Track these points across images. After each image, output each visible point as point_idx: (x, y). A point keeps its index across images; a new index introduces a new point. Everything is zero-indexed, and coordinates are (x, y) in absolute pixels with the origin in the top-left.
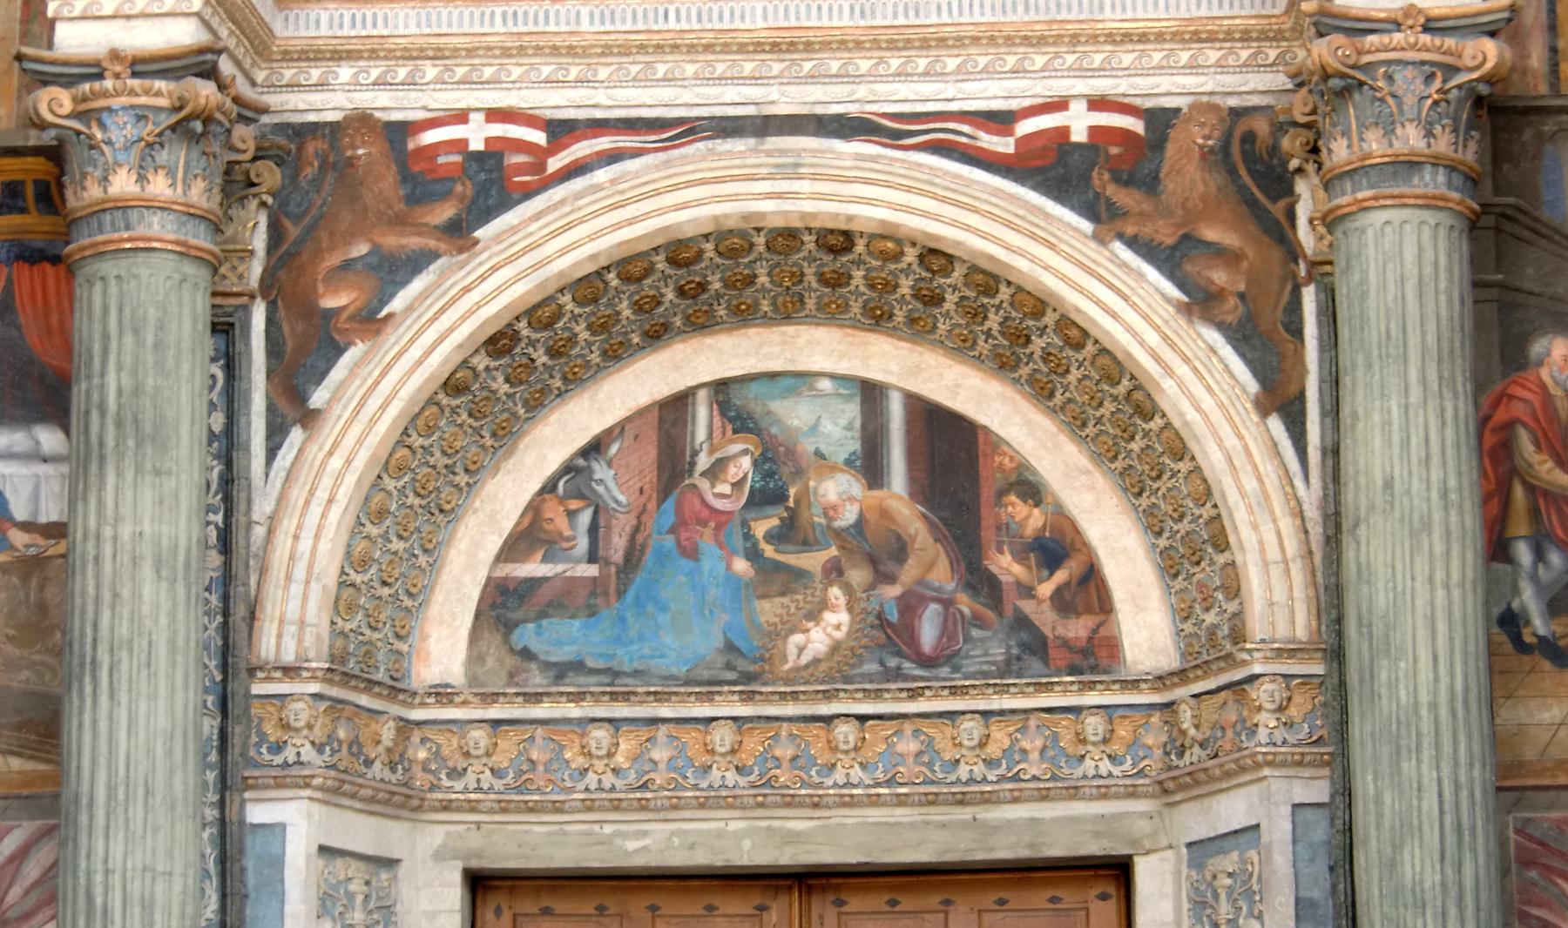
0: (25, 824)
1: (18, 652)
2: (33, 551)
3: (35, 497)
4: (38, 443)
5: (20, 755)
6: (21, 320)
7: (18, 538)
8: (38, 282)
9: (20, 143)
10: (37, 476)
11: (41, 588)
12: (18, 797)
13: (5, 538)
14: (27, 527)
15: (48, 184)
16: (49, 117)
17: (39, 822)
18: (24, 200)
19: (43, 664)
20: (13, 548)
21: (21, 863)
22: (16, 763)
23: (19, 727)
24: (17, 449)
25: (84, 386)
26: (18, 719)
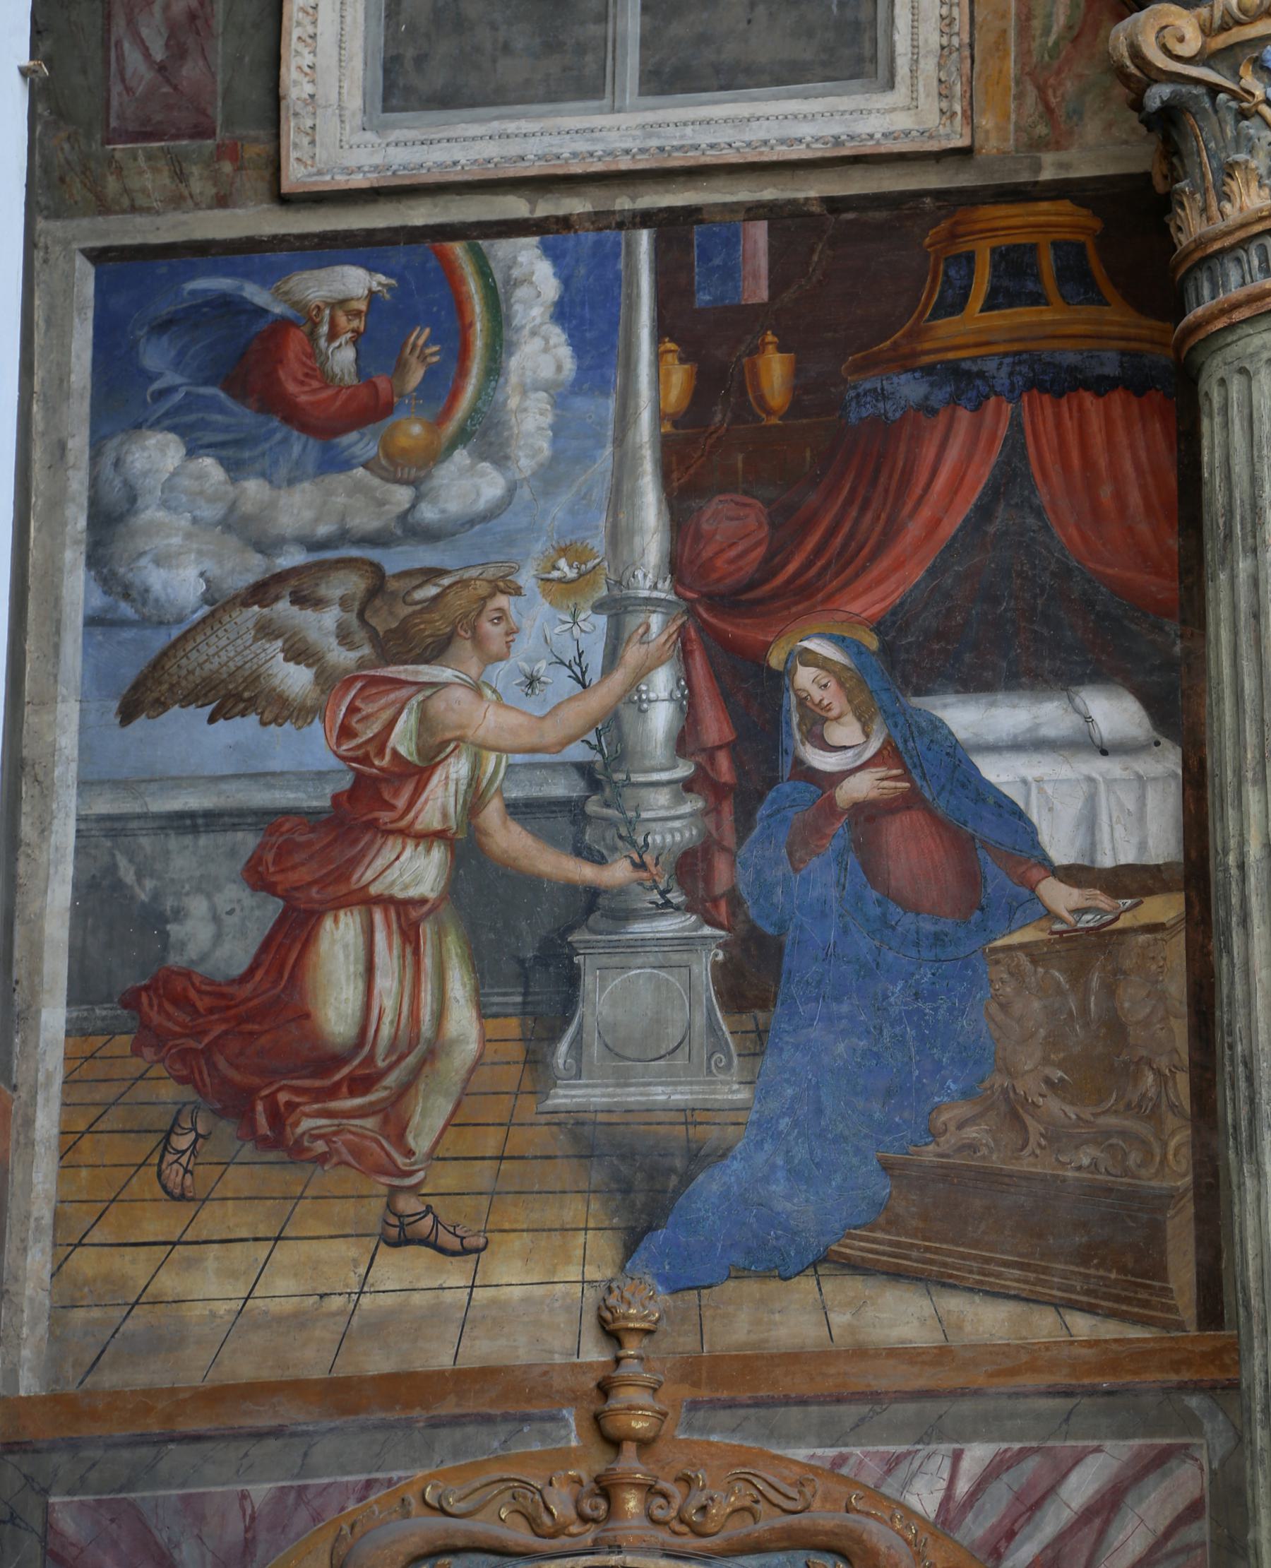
0: (1108, 1444)
1: (1072, 1112)
2: (1088, 920)
3: (1090, 821)
4: (1088, 719)
5: (1090, 1310)
6: (1043, 497)
7: (1060, 896)
8: (1069, 425)
9: (1024, 177)
10: (1090, 780)
11: (1110, 990)
12: (1092, 1392)
13: (1035, 898)
14: (1074, 875)
15: (1081, 246)
16: (1162, 61)
17: (1137, 1442)
18: (1038, 278)
19: (1123, 1133)
20: (1051, 915)
21: (1107, 1523)
22: (1082, 1325)
23: (1084, 1256)
24: (1049, 732)
25: (1244, 566)
26: (1080, 1239)
